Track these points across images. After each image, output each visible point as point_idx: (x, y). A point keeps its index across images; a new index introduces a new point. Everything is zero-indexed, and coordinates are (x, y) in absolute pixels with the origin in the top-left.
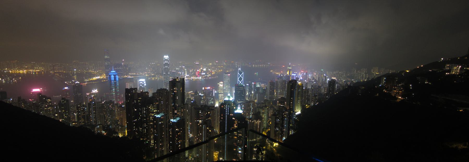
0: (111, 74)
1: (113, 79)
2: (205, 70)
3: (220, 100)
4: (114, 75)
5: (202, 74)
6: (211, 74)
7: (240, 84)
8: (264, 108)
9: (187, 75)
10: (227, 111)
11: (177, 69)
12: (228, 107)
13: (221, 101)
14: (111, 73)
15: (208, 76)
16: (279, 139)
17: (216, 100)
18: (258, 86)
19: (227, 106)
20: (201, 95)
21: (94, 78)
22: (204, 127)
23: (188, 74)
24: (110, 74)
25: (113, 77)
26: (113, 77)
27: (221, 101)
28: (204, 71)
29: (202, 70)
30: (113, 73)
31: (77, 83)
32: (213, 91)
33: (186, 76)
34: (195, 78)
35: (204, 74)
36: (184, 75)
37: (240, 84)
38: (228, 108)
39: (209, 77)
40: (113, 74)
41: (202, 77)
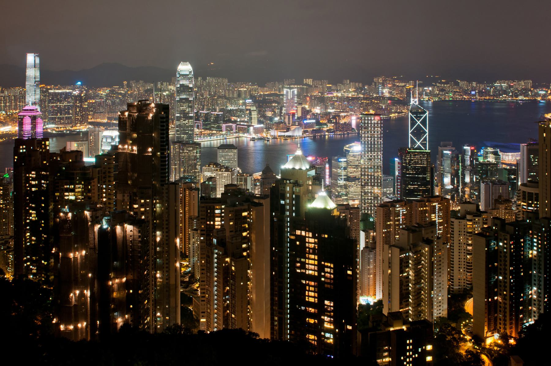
0: (25, 114)
2: (317, 110)
4: (34, 118)
5: (305, 122)
6: (336, 123)
7: (416, 149)
8: (468, 217)
9: (255, 126)
11: (230, 108)
14: (27, 110)
15: (325, 129)
16: (508, 322)
23: (260, 122)
24: (21, 114)
25: (27, 121)
26: (27, 121)
28: (313, 114)
29: (305, 112)
30: (31, 110)
32: (324, 169)
33: (254, 129)
34: (283, 134)
35: (314, 121)
36: (250, 124)
37: (419, 148)
39: (328, 131)
40: (30, 114)
41: (305, 132)
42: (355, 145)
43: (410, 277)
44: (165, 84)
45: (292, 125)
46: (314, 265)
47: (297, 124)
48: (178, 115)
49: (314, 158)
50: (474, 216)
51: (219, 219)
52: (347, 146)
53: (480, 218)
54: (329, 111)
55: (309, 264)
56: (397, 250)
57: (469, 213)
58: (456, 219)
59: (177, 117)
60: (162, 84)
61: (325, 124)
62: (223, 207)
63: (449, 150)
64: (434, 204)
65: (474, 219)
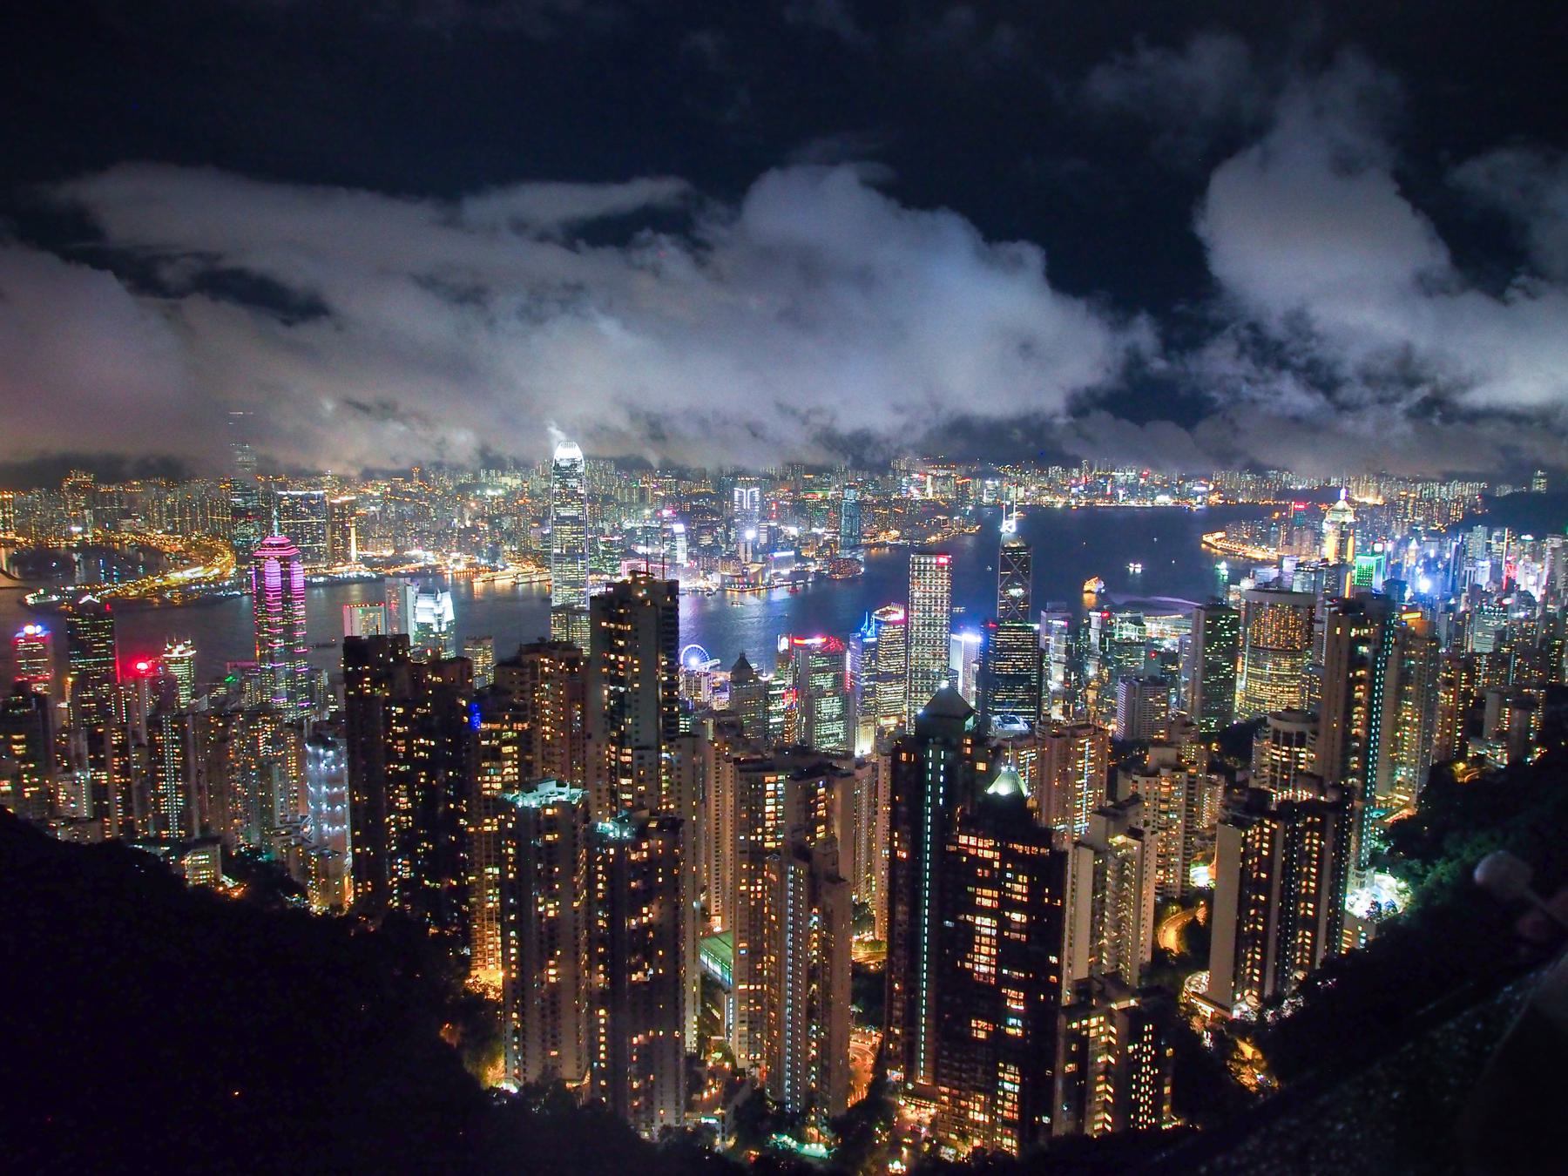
1: (274, 581)
2: (793, 531)
3: (887, 717)
4: (285, 561)
8: (1164, 772)
10: (936, 784)
11: (627, 525)
12: (937, 762)
13: (893, 721)
14: (271, 545)
17: (861, 719)
18: (1129, 632)
19: (936, 754)
20: (774, 683)
21: (176, 577)
22: (791, 876)
27: (893, 721)
29: (774, 534)
31: (90, 601)
38: (942, 767)
42: (894, 612)
43: (1107, 901)
44: (493, 472)
45: (752, 562)
46: (992, 898)
47: (760, 561)
48: (558, 551)
49: (825, 640)
50: (1174, 770)
51: (772, 801)
52: (877, 612)
53: (1184, 775)
54: (814, 530)
55: (982, 896)
56: (1092, 852)
57: (1165, 765)
58: (1142, 776)
59: (556, 555)
60: (488, 474)
61: (812, 559)
62: (780, 777)
63: (1063, 619)
64: (1082, 741)
65: (1174, 777)
